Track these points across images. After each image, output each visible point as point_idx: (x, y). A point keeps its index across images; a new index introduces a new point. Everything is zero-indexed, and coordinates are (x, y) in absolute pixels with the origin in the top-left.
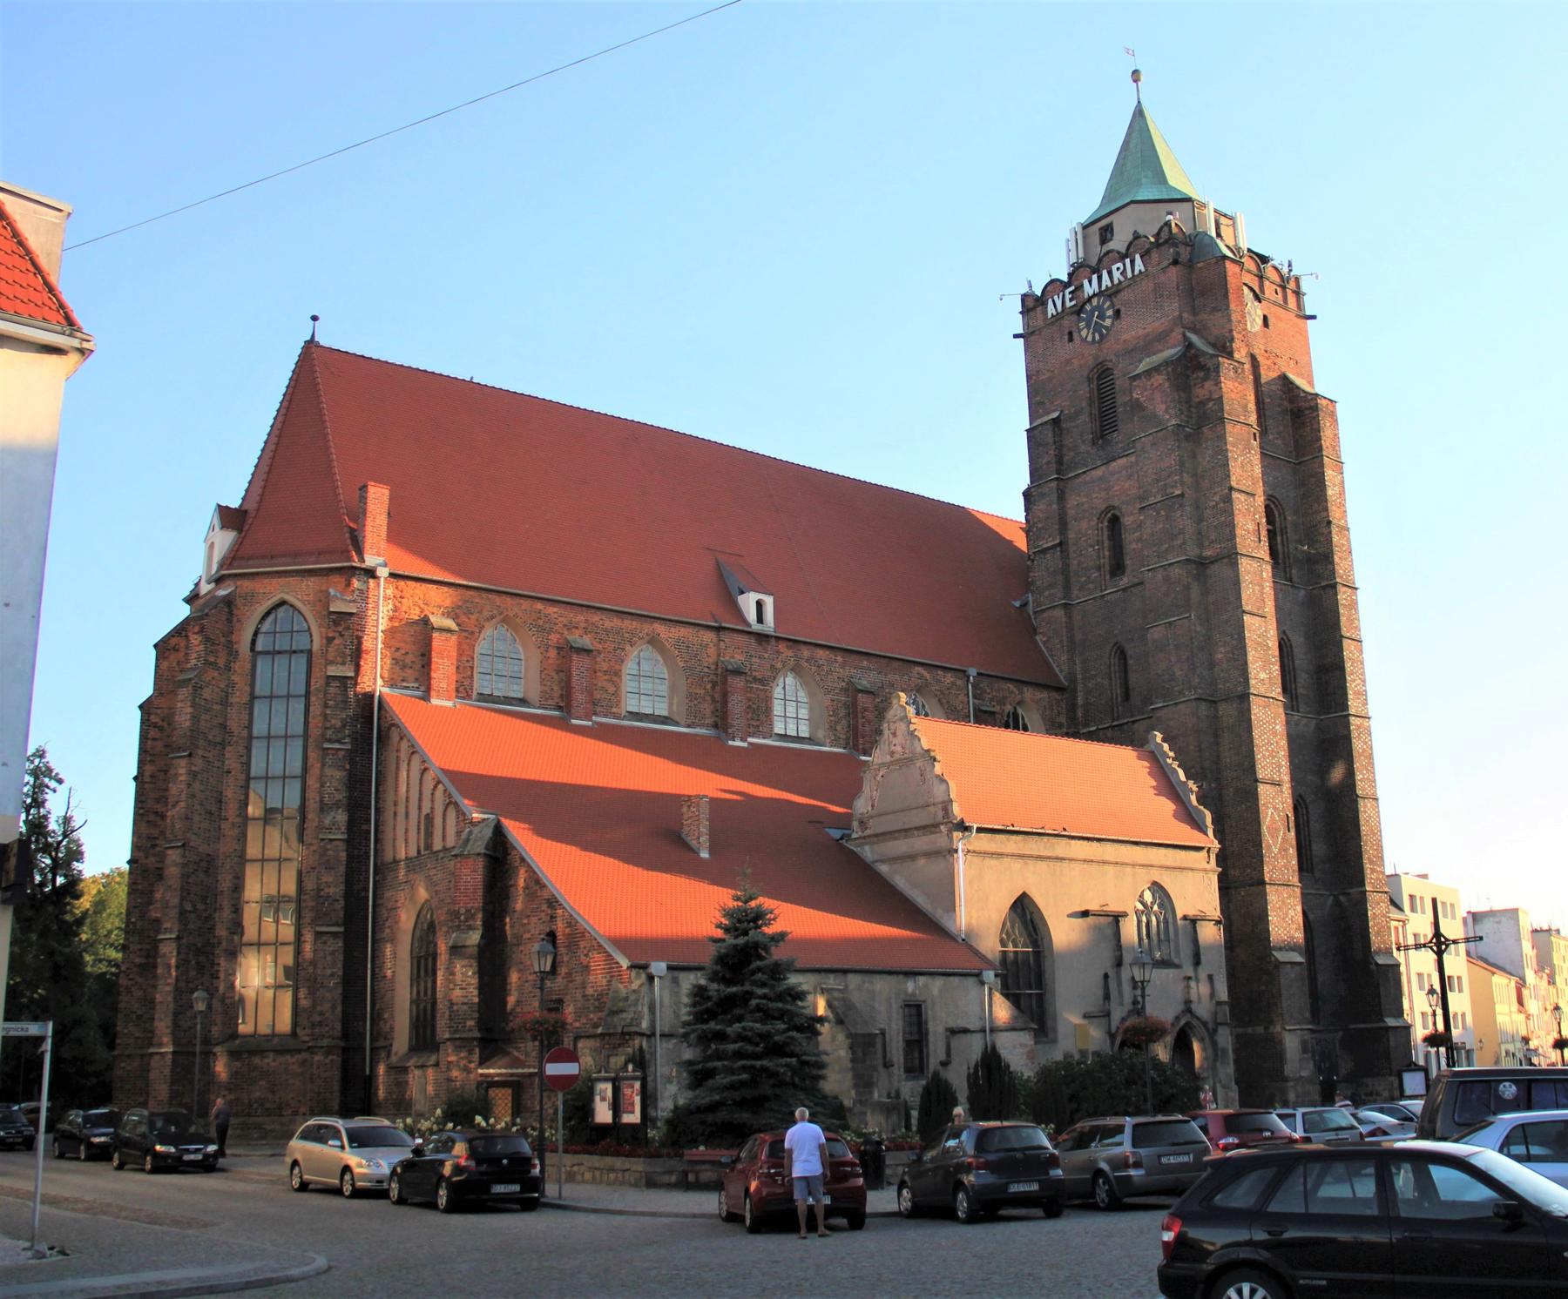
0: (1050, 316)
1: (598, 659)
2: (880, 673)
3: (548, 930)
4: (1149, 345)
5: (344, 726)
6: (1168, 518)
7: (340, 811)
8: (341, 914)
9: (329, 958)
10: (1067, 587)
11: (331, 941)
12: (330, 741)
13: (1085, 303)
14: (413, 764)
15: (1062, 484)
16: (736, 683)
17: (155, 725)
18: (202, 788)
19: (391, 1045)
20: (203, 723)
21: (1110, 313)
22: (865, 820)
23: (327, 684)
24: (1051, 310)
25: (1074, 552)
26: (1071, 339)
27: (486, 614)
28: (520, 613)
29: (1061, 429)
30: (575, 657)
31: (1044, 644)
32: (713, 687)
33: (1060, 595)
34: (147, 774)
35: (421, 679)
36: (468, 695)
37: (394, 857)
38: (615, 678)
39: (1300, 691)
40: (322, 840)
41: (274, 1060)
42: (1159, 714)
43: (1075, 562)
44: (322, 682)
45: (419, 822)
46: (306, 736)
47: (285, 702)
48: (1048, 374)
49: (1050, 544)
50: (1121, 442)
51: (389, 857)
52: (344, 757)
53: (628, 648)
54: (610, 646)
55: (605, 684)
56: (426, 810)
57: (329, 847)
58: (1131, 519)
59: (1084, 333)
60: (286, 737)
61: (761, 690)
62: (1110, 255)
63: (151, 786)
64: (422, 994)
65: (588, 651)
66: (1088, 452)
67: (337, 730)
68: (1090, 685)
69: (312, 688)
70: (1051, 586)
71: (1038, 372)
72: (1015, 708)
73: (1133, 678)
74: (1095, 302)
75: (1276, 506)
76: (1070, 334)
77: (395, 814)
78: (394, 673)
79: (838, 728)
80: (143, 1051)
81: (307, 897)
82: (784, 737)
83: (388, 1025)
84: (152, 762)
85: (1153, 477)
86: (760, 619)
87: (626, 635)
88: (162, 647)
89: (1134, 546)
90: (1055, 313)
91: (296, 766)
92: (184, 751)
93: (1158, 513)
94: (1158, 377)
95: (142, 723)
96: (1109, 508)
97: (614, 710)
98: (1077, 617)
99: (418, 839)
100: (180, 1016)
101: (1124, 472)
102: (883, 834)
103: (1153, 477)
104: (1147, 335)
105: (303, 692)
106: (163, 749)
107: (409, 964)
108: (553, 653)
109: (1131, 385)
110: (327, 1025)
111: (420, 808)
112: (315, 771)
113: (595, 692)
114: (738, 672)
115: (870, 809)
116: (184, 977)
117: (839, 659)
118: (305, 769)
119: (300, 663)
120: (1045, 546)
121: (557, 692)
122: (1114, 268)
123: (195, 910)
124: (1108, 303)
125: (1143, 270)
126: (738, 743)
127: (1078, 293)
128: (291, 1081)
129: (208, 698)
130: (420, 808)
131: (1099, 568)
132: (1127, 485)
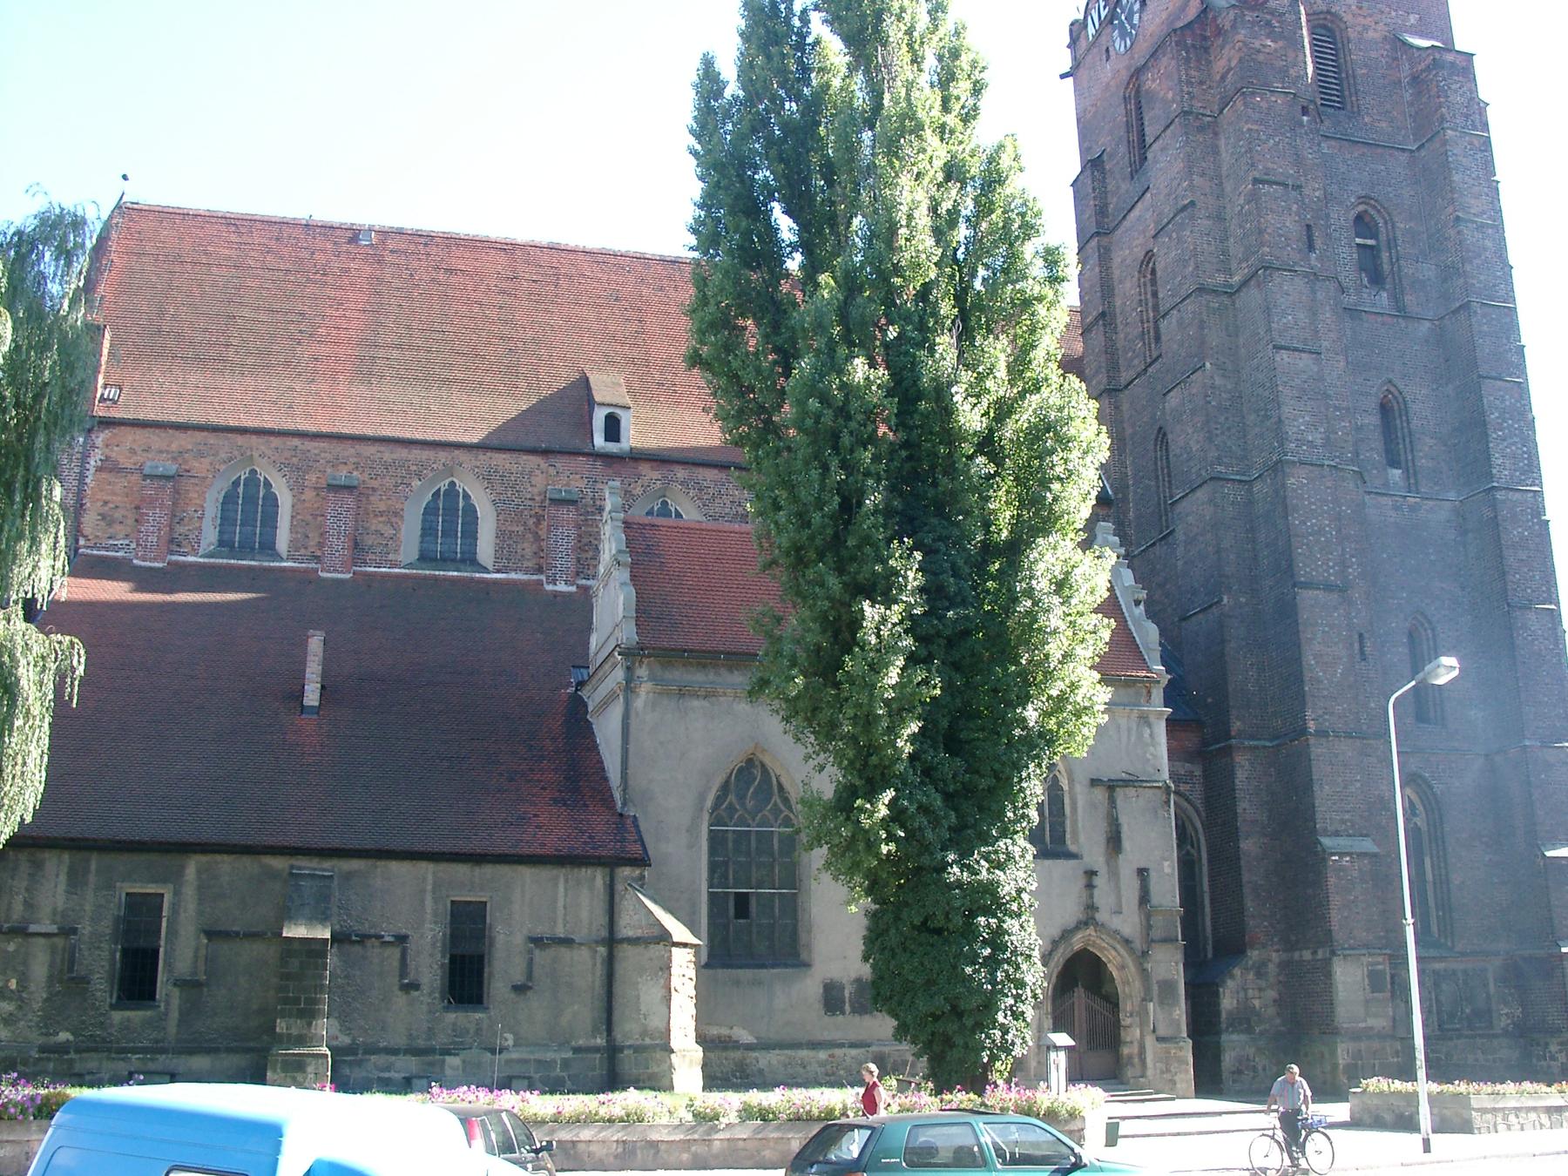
1: (372, 498)
15: (1105, 241)
29: (1103, 172)
36: (194, 550)
38: (394, 520)
39: (1423, 462)
54: (389, 482)
65: (350, 488)
75: (1379, 211)
87: (414, 468)
97: (391, 557)
108: (309, 495)
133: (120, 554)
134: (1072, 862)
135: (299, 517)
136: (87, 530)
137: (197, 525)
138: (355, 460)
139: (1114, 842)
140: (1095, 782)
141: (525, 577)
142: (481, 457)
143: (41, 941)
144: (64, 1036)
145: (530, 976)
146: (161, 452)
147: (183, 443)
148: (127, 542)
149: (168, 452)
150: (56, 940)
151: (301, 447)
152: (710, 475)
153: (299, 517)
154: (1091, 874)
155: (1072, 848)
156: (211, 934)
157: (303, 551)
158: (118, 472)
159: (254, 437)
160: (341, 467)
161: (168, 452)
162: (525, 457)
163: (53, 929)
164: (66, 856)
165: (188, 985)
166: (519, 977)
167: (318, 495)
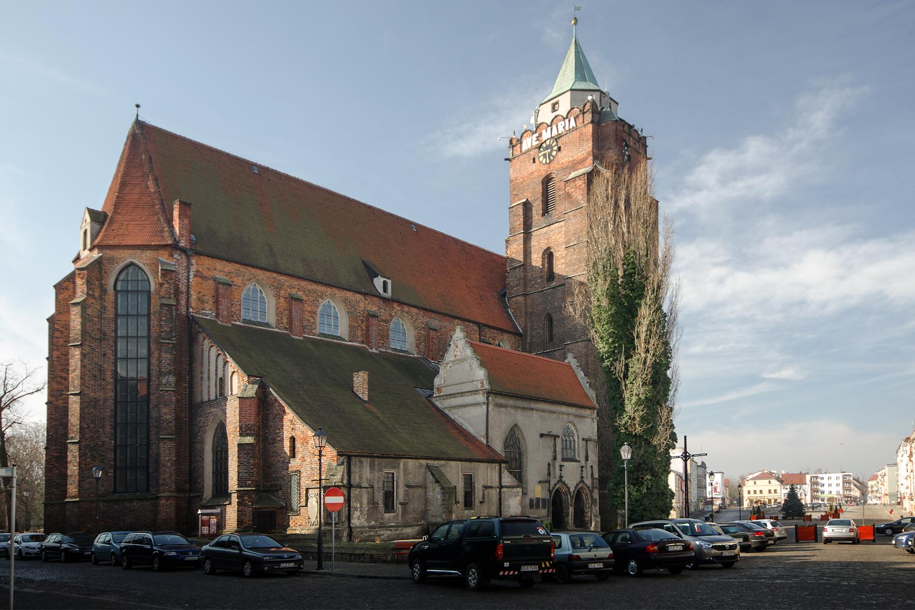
2: (440, 321)
3: (291, 435)
4: (574, 165)
5: (172, 331)
6: (579, 252)
7: (171, 376)
8: (174, 429)
9: (167, 451)
10: (525, 286)
11: (168, 443)
12: (164, 339)
13: (543, 143)
14: (211, 352)
16: (374, 321)
17: (58, 330)
18: (89, 362)
19: (202, 495)
20: (87, 327)
21: (556, 148)
22: (440, 388)
23: (161, 308)
24: (524, 148)
25: (530, 269)
26: (534, 162)
27: (246, 277)
28: (265, 279)
30: (294, 302)
31: (512, 313)
32: (362, 323)
33: (522, 290)
34: (55, 356)
35: (213, 309)
37: (202, 400)
38: (314, 315)
40: (162, 390)
41: (137, 504)
42: (569, 346)
43: (530, 274)
44: (158, 308)
45: (216, 382)
46: (149, 337)
47: (136, 318)
48: (522, 180)
49: (518, 265)
50: (557, 215)
51: (198, 400)
52: (172, 347)
53: (320, 300)
54: (311, 299)
55: (309, 318)
56: (220, 375)
57: (166, 394)
58: (559, 253)
59: (541, 159)
60: (127, 337)
61: (385, 326)
62: (558, 117)
63: (57, 362)
64: (219, 469)
65: (301, 300)
66: (539, 220)
67: (167, 334)
68: (534, 333)
69: (152, 311)
70: (517, 285)
71: (516, 178)
72: (499, 343)
73: (555, 331)
74: (548, 142)
76: (534, 159)
77: (202, 378)
78: (198, 305)
79: (420, 346)
80: (61, 502)
81: (153, 420)
82: (395, 350)
83: (200, 485)
84: (57, 350)
85: (573, 232)
86: (385, 290)
87: (319, 294)
88: (59, 287)
89: (560, 266)
91: (144, 352)
92: (77, 342)
93: (574, 250)
94: (579, 181)
95: (50, 328)
96: (549, 248)
97: (314, 331)
98: (529, 301)
99: (216, 391)
100: (83, 483)
101: (557, 230)
102: (450, 395)
103: (573, 232)
104: (574, 161)
105: (146, 313)
106: (63, 343)
107: (211, 455)
108: (282, 300)
109: (565, 185)
110: (167, 486)
111: (216, 374)
112: (156, 354)
113: (304, 322)
114: (374, 316)
115: (443, 382)
116: (84, 462)
117: (421, 313)
118: (149, 354)
119: (142, 299)
120: (515, 266)
121: (285, 321)
123: (89, 427)
124: (555, 143)
126: (374, 350)
127: (540, 138)
128: (147, 514)
129: (91, 314)
130: (216, 374)
131: (541, 278)
132: (558, 237)
133: (208, 317)
134: (578, 463)
135: (279, 310)
136: (193, 305)
137: (239, 308)
138: (298, 287)
139: (587, 459)
140: (583, 439)
141: (359, 345)
142: (342, 292)
143: (364, 490)
144: (373, 523)
145: (484, 498)
146: (220, 271)
147: (230, 268)
148: (210, 312)
149: (224, 272)
150: (368, 489)
151: (278, 278)
152: (414, 310)
153: (279, 310)
154: (582, 467)
155: (578, 459)
156: (408, 486)
157: (281, 325)
158: (204, 278)
159: (258, 270)
160: (293, 289)
161: (224, 272)
162: (357, 295)
163: (367, 485)
164: (369, 459)
165: (403, 504)
166: (481, 499)
167: (285, 300)
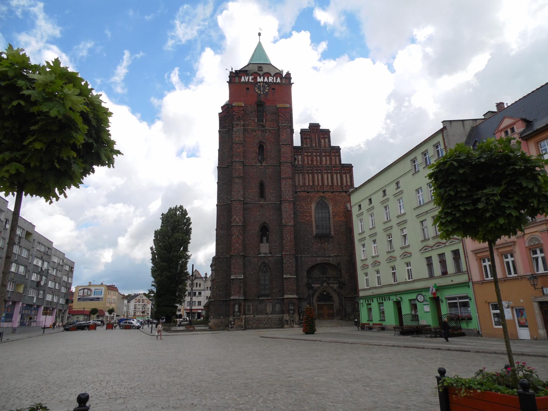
0: (242, 81)
90: (244, 81)
122: (270, 78)
125: (280, 82)
